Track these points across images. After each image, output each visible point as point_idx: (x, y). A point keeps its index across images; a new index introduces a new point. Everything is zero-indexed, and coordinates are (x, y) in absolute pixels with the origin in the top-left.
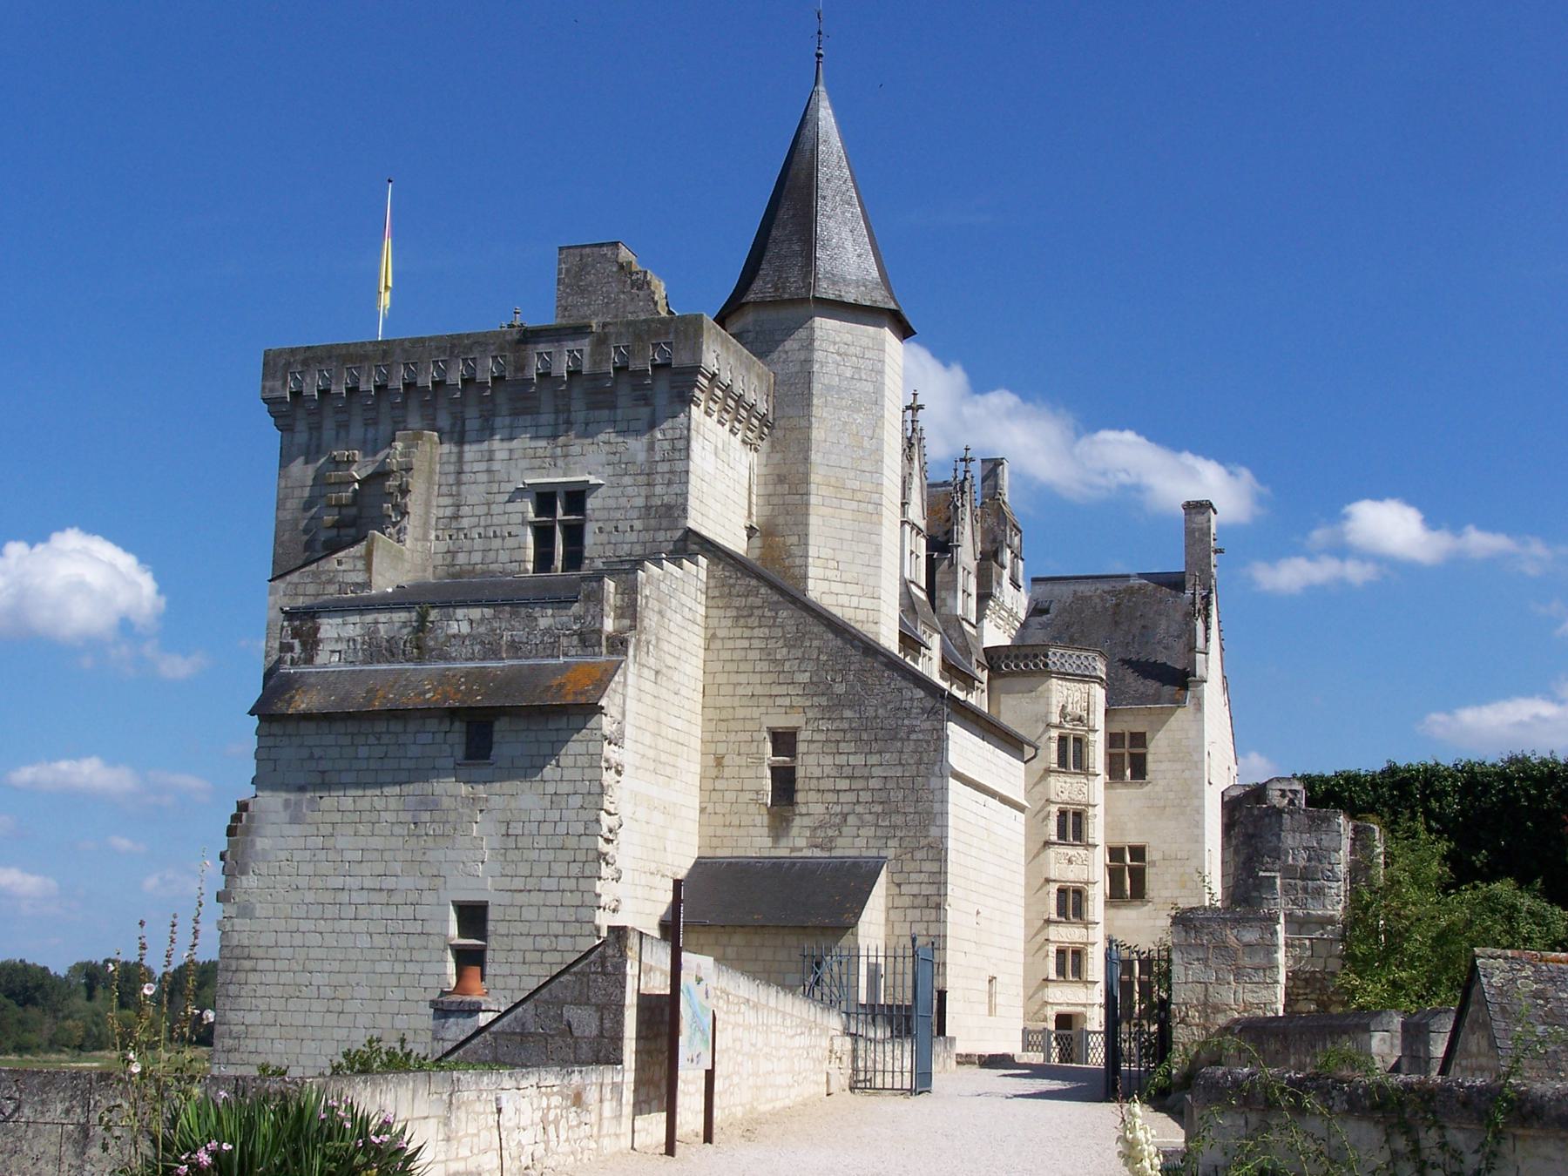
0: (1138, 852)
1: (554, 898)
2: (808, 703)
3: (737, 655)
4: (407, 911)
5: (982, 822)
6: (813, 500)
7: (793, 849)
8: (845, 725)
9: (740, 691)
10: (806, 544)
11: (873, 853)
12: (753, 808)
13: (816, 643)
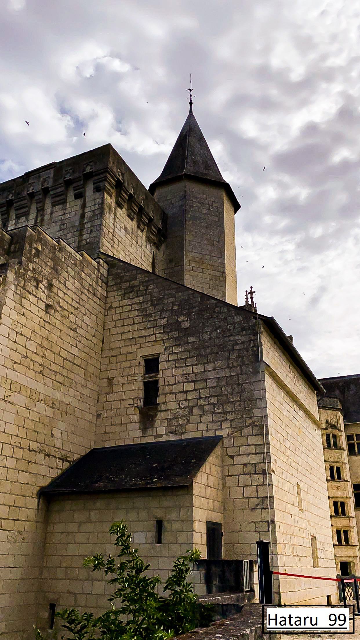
2: (166, 337)
3: (123, 316)
5: (294, 421)
6: (187, 268)
7: (156, 436)
8: (190, 347)
9: (125, 337)
11: (211, 434)
12: (130, 411)
13: (171, 300)
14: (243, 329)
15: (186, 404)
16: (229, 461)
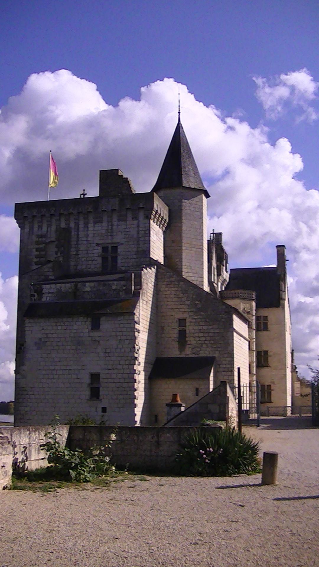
0: (266, 352)
1: (122, 371)
4: (74, 376)
5: (240, 345)
6: (184, 248)
7: (186, 355)
10: (182, 262)
14: (226, 312)
15: (200, 342)
16: (218, 366)
